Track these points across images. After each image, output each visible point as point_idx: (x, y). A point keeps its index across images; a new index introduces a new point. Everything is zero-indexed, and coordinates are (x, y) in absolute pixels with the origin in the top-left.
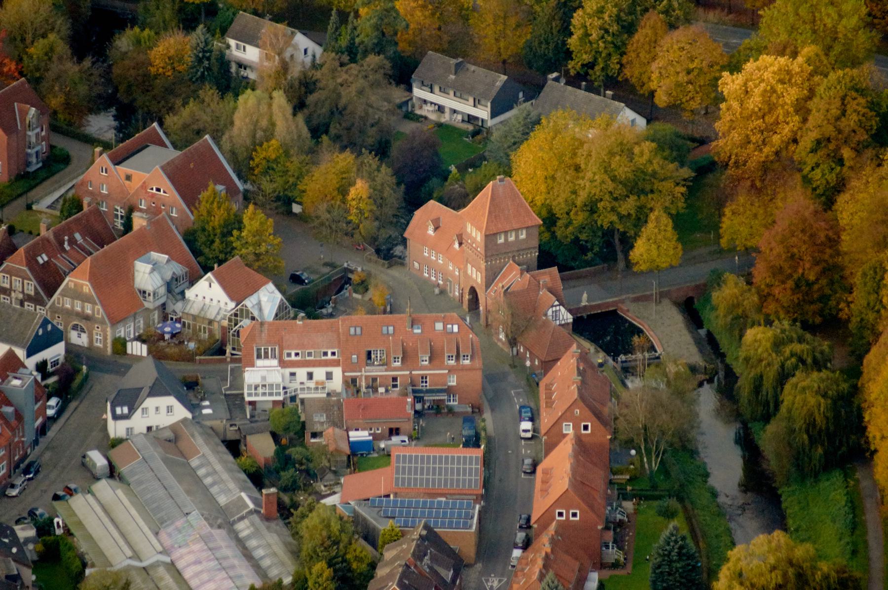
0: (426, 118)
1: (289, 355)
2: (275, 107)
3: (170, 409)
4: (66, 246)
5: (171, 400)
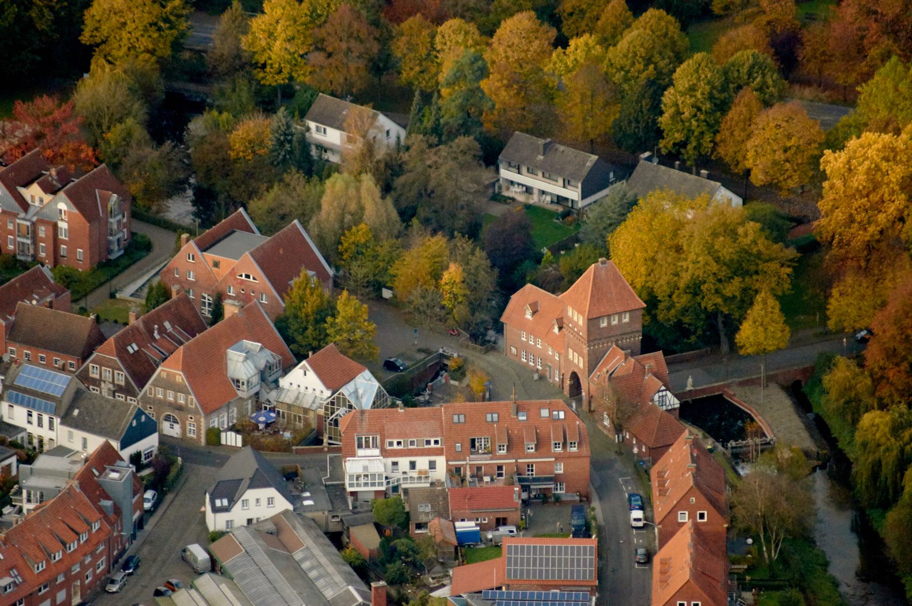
0: (513, 199)
1: (391, 444)
3: (270, 501)
4: (156, 335)
5: (272, 492)
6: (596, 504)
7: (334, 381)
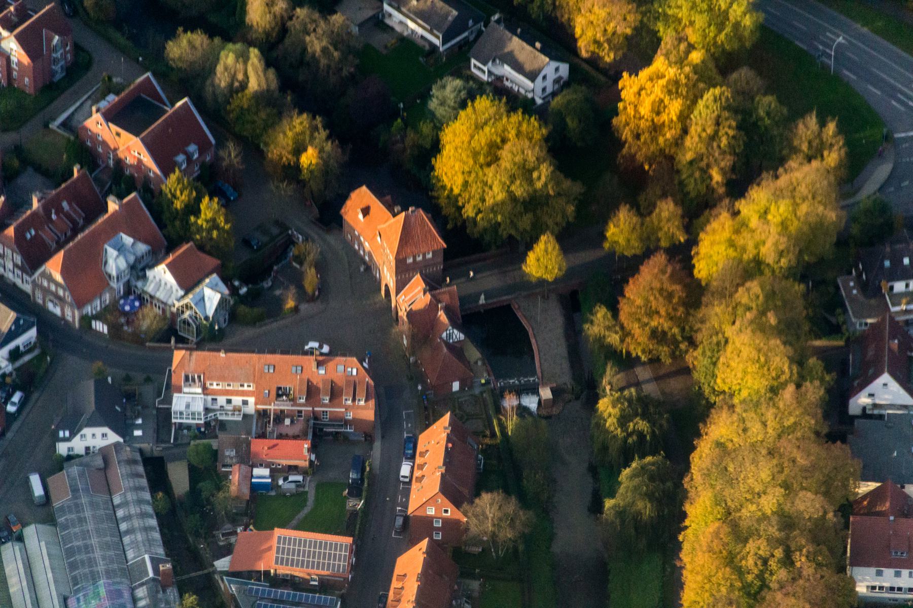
0: (392, 29)
1: (211, 384)
2: (250, 69)
4: (54, 217)
5: (106, 430)
6: (377, 445)
7: (188, 283)
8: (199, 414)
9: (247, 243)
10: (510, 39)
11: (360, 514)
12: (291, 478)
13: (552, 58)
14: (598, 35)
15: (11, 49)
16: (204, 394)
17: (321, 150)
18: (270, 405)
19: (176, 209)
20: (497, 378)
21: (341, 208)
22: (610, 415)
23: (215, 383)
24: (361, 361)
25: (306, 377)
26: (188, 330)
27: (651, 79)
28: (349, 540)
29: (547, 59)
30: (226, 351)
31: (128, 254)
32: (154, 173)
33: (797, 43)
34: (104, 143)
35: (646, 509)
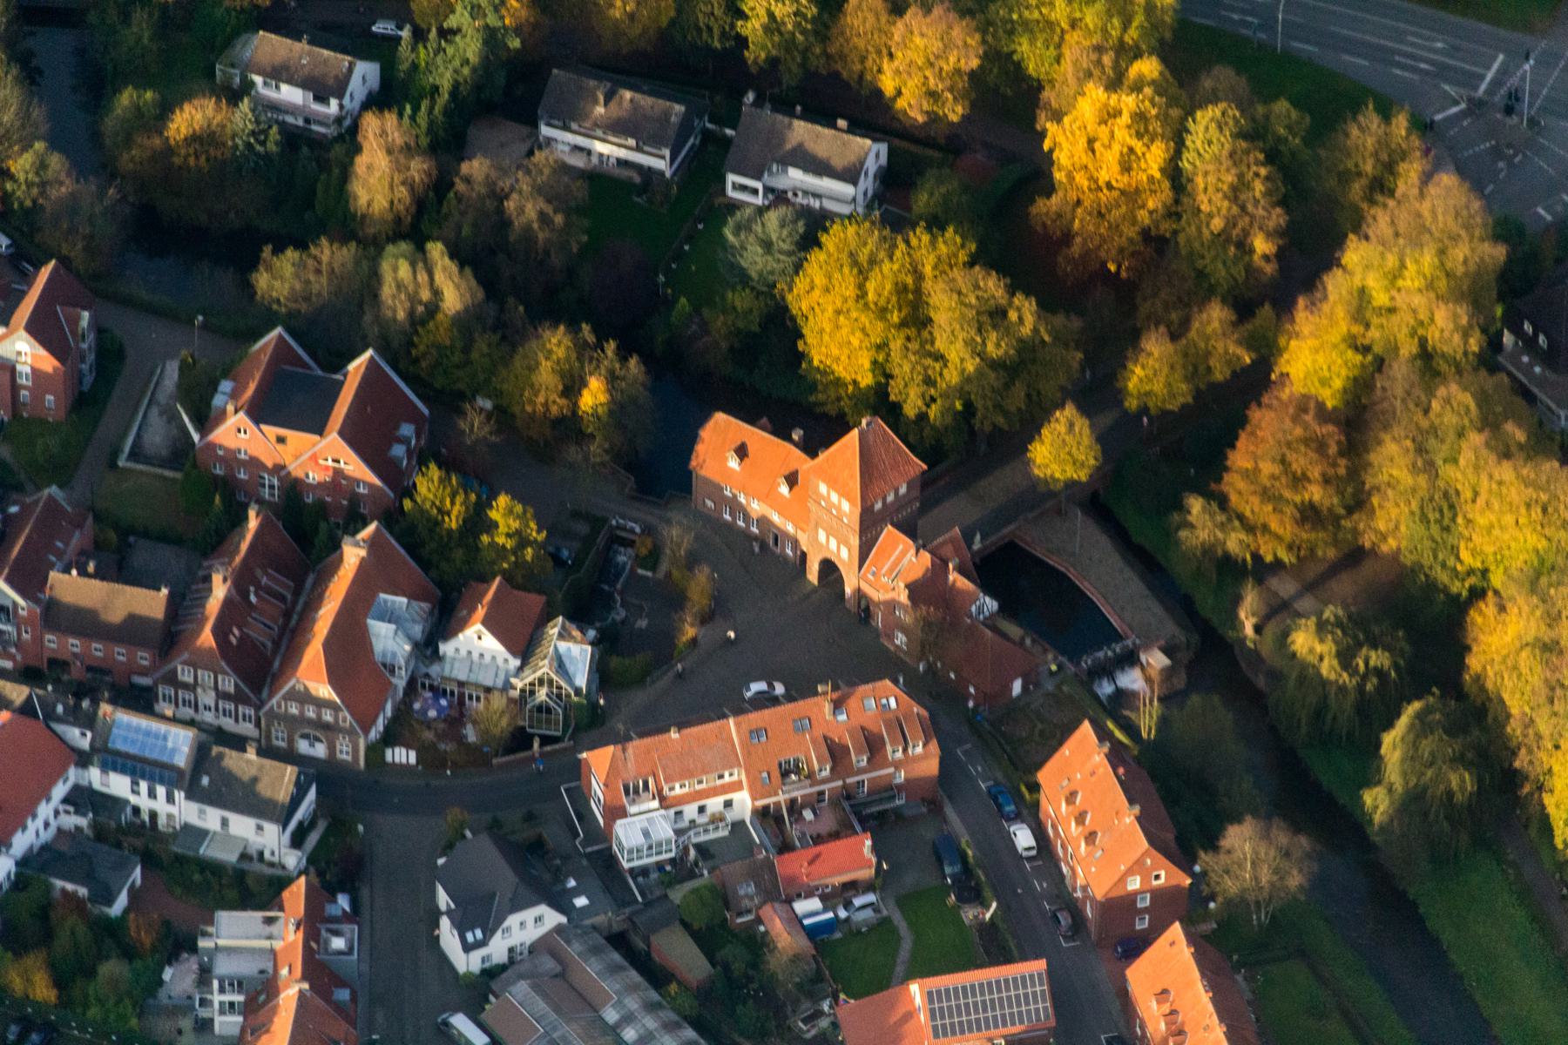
1: (672, 789)
3: (538, 920)
4: (253, 598)
5: (543, 909)
6: (949, 811)
7: (525, 647)
8: (668, 842)
9: (558, 561)
10: (790, 125)
11: (1001, 925)
12: (858, 902)
13: (874, 140)
14: (932, 81)
15: (19, 353)
16: (662, 807)
17: (612, 379)
18: (776, 794)
19: (450, 531)
20: (1075, 657)
21: (689, 459)
22: (1321, 659)
23: (677, 786)
24: (895, 682)
25: (819, 733)
26: (548, 722)
27: (1103, 122)
28: (1040, 965)
29: (868, 142)
30: (681, 727)
31: (408, 625)
32: (371, 486)
33: (1198, 20)
34: (254, 463)
35: (1461, 782)
